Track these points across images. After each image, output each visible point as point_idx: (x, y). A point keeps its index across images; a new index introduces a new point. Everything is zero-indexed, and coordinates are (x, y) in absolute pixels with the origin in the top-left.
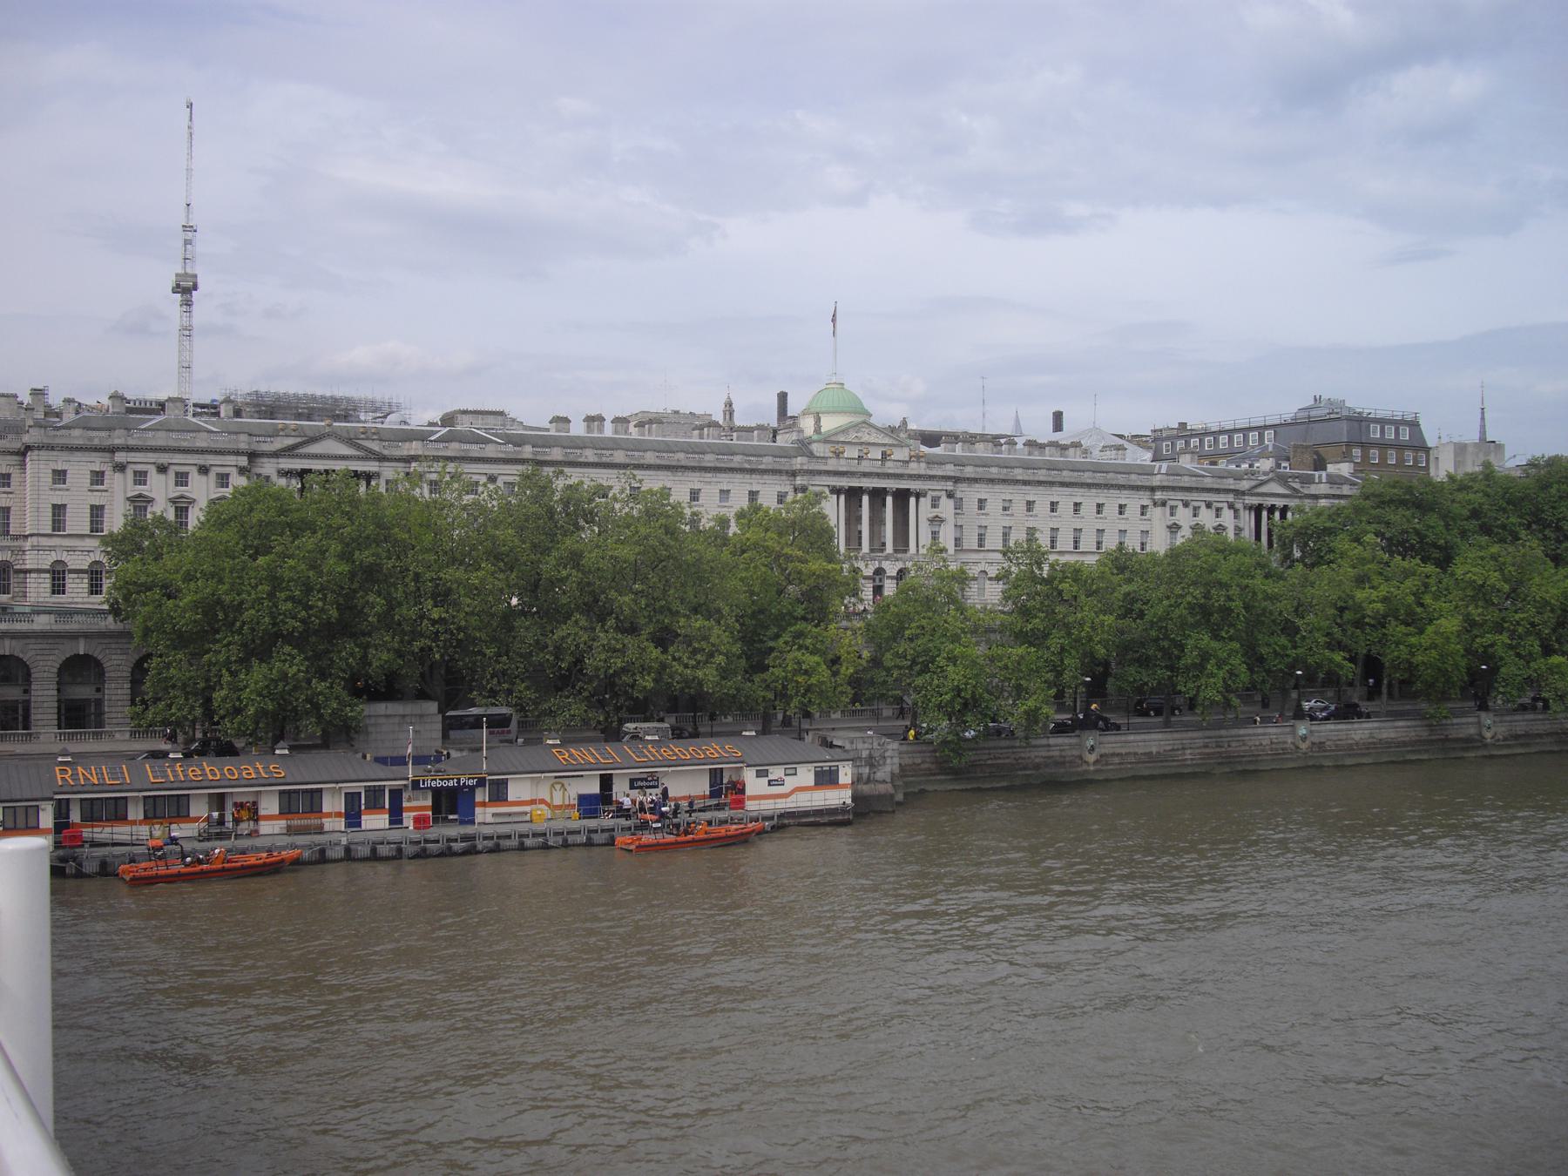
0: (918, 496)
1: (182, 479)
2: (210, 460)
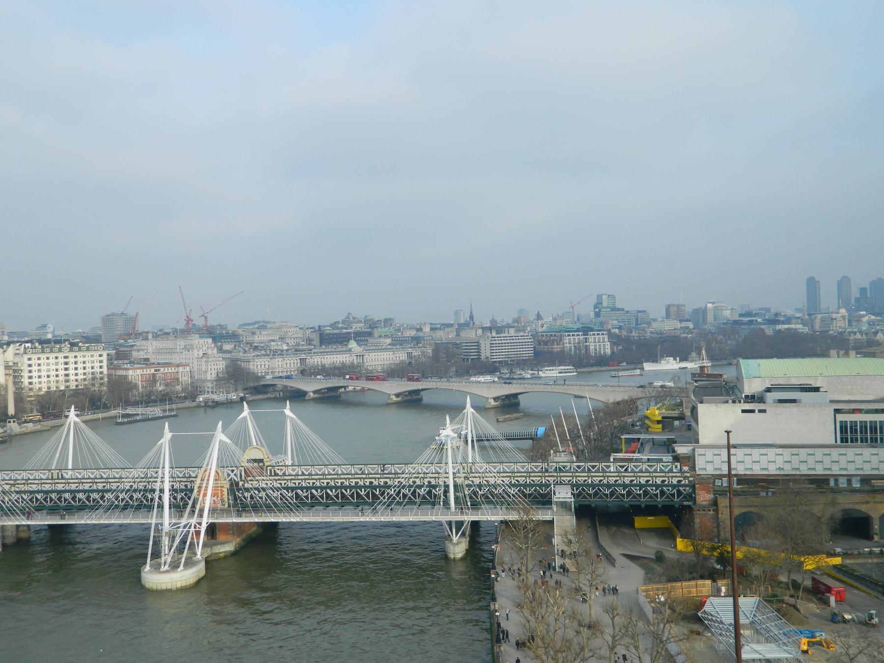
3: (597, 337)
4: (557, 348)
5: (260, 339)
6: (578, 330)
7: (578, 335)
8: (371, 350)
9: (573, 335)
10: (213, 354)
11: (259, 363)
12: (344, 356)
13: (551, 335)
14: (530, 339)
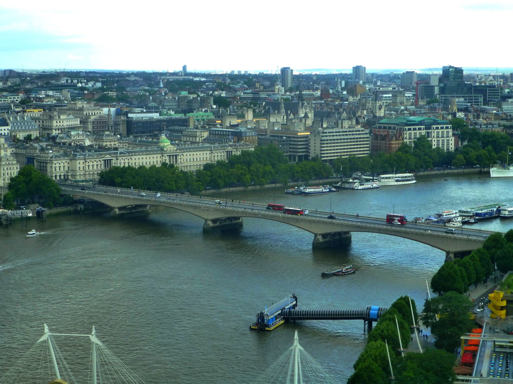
0: (178, 155)
1: (93, 162)
2: (96, 160)
3: (440, 131)
4: (396, 144)
5: (58, 124)
6: (420, 123)
7: (420, 129)
8: (187, 149)
9: (415, 129)
10: (6, 155)
11: (58, 165)
12: (155, 156)
13: (390, 128)
14: (366, 134)
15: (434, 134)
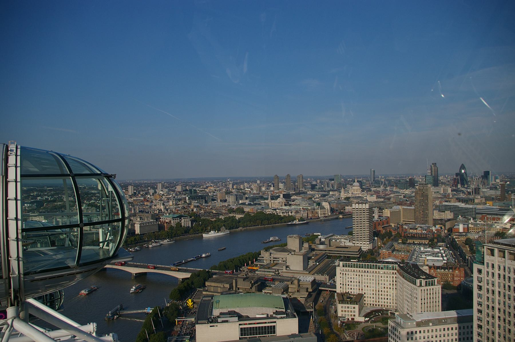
6: (178, 217)
7: (177, 219)
9: (175, 219)
15: (183, 221)
